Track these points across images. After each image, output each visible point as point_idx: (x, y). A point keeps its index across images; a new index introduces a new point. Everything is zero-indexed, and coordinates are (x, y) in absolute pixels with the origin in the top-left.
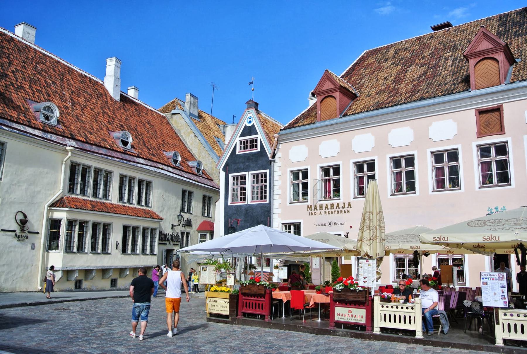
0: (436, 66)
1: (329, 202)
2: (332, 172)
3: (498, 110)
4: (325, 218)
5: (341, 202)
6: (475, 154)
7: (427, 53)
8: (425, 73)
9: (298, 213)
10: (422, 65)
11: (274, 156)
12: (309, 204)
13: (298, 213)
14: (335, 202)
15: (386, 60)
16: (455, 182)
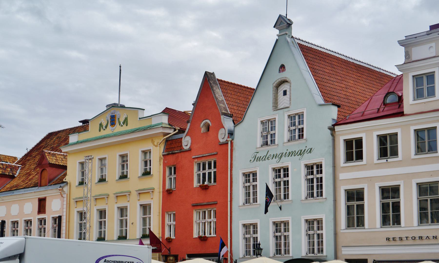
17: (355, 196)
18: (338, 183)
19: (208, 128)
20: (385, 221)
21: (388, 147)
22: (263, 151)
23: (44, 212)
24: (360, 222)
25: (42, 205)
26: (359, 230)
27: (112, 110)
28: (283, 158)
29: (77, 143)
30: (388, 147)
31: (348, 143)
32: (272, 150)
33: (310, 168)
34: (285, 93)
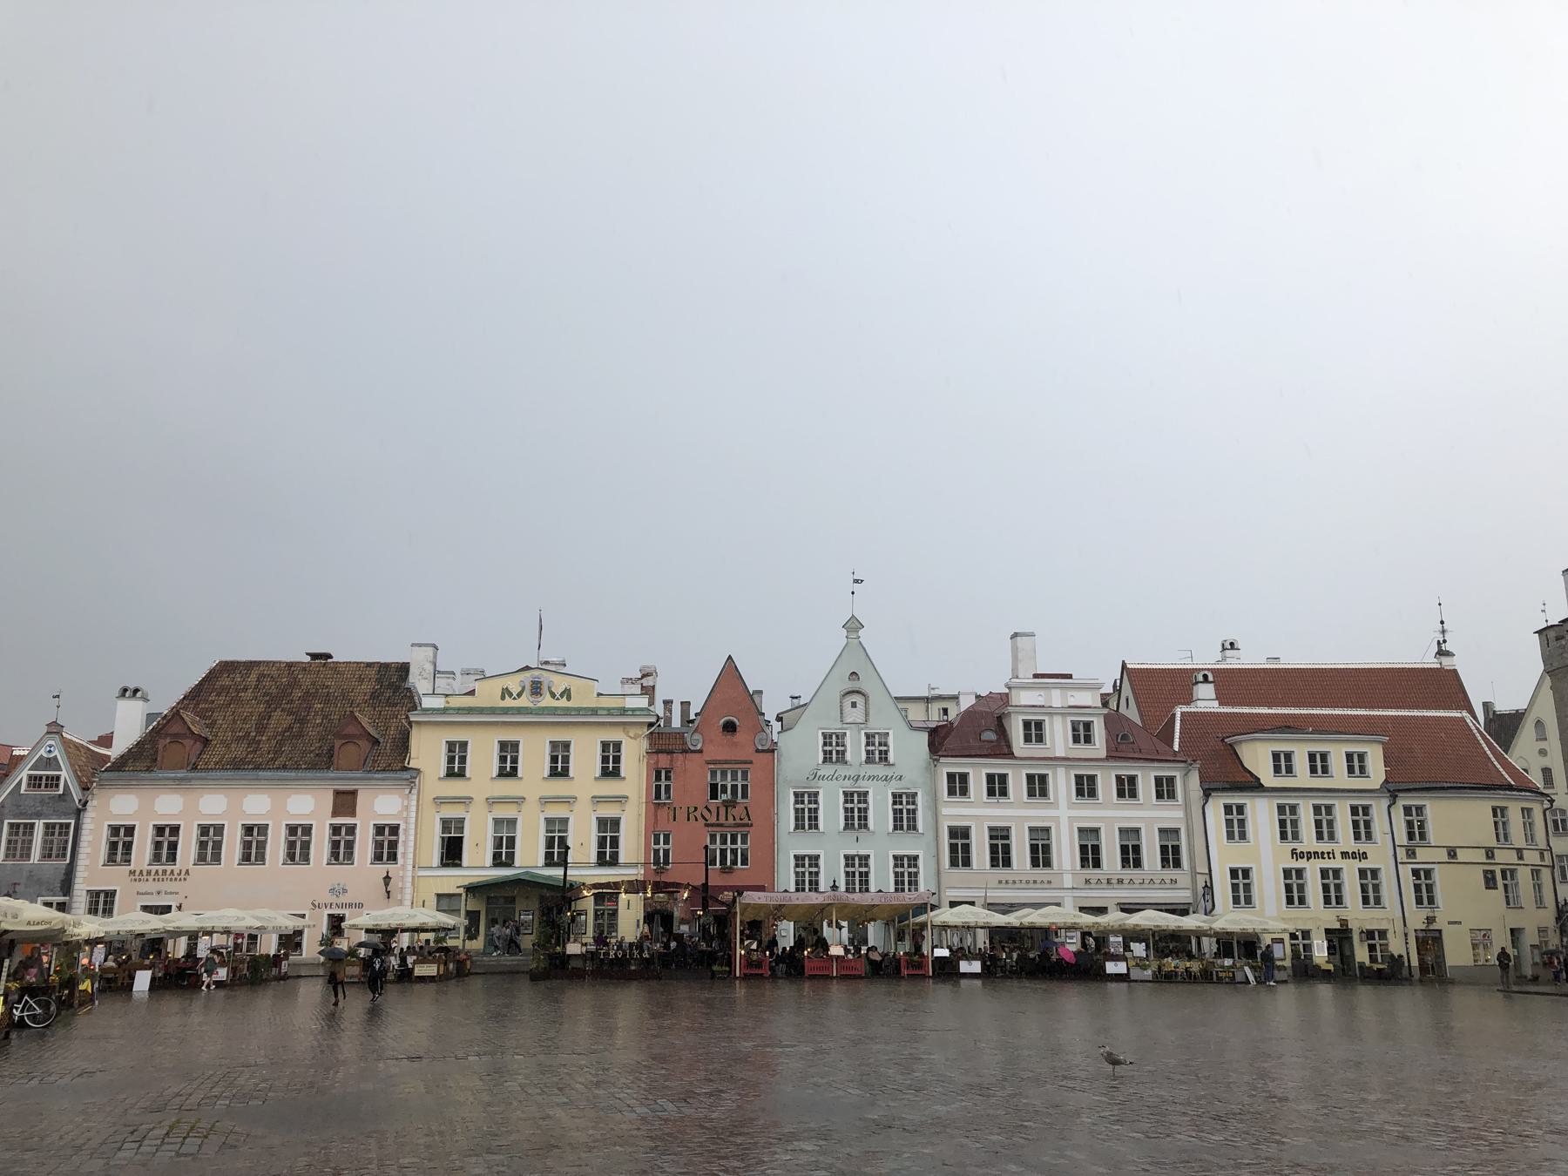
0: (302, 721)
1: (160, 868)
2: (166, 836)
3: (354, 793)
4: (151, 886)
5: (176, 868)
6: (327, 831)
7: (297, 694)
8: (290, 728)
9: (114, 878)
10: (290, 713)
11: (85, 804)
12: (132, 867)
13: (114, 878)
14: (169, 868)
15: (245, 689)
16: (306, 858)
17: (960, 834)
18: (940, 819)
19: (730, 727)
20: (994, 862)
21: (997, 786)
22: (828, 770)
23: (353, 814)
24: (967, 863)
25: (345, 802)
26: (965, 870)
27: (536, 673)
28: (860, 783)
29: (444, 711)
30: (997, 786)
31: (951, 776)
32: (842, 770)
33: (897, 798)
34: (854, 705)
